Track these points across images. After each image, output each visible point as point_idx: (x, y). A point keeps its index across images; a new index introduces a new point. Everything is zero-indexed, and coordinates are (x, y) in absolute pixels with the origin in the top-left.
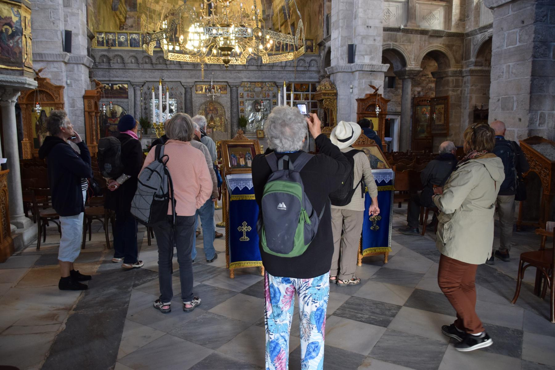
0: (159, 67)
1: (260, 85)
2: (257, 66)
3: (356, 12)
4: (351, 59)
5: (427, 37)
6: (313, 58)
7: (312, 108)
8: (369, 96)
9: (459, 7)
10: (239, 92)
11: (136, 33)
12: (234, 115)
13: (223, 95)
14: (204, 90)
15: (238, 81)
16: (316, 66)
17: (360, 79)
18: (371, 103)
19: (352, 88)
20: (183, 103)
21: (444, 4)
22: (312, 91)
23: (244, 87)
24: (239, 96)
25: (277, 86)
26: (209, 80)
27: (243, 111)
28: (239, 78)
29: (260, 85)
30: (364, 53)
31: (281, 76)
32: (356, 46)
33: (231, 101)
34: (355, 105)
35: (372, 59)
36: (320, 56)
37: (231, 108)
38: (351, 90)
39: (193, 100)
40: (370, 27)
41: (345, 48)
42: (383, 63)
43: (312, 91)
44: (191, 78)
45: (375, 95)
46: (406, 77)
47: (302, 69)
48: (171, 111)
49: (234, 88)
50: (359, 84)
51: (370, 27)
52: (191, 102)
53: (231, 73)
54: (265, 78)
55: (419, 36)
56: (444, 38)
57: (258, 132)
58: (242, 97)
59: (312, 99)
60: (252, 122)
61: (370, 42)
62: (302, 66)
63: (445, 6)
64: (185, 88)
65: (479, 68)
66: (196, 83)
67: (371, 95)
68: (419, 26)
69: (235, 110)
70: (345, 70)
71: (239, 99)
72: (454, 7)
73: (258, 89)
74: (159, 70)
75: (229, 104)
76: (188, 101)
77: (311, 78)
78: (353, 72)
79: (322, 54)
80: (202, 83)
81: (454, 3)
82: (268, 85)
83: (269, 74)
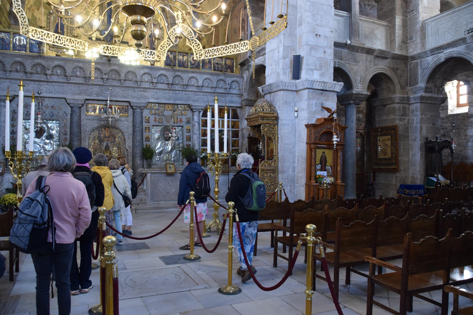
0: (36, 77)
1: (171, 108)
2: (168, 84)
3: (301, 17)
4: (296, 75)
5: (372, 57)
6: (235, 79)
7: (233, 137)
8: (322, 121)
9: (401, 28)
10: (144, 115)
11: (5, 32)
12: (137, 144)
13: (123, 119)
14: (97, 111)
15: (144, 101)
16: (237, 88)
17: (309, 99)
18: (324, 130)
19: (297, 111)
20: (69, 127)
21: (386, 24)
22: (232, 118)
23: (151, 109)
24: (144, 120)
25: (192, 110)
26: (105, 99)
27: (148, 139)
28: (145, 97)
29: (171, 108)
30: (313, 67)
31: (196, 98)
32: (302, 58)
33: (134, 126)
34: (304, 133)
35: (322, 75)
36: (242, 77)
37: (133, 135)
38: (296, 114)
39: (82, 123)
40: (320, 36)
41: (289, 61)
42: (334, 80)
43: (232, 118)
44: (80, 94)
45: (330, 120)
46: (352, 102)
47: (222, 91)
48: (50, 137)
49: (138, 110)
50: (309, 105)
51: (320, 36)
52: (80, 126)
53: (134, 91)
54: (178, 99)
55: (364, 55)
56: (389, 60)
57: (168, 166)
58: (148, 121)
59: (233, 127)
60: (160, 153)
61: (321, 55)
62: (221, 88)
63: (387, 26)
64: (72, 107)
65: (428, 95)
66: (87, 102)
67: (325, 119)
68: (364, 44)
69: (138, 138)
70: (289, 88)
71: (144, 123)
72: (397, 27)
73: (168, 113)
74: (35, 81)
75: (131, 130)
76: (75, 125)
77: (231, 102)
78: (297, 91)
79: (245, 75)
80: (96, 102)
81: (397, 23)
82: (180, 108)
83: (181, 95)
